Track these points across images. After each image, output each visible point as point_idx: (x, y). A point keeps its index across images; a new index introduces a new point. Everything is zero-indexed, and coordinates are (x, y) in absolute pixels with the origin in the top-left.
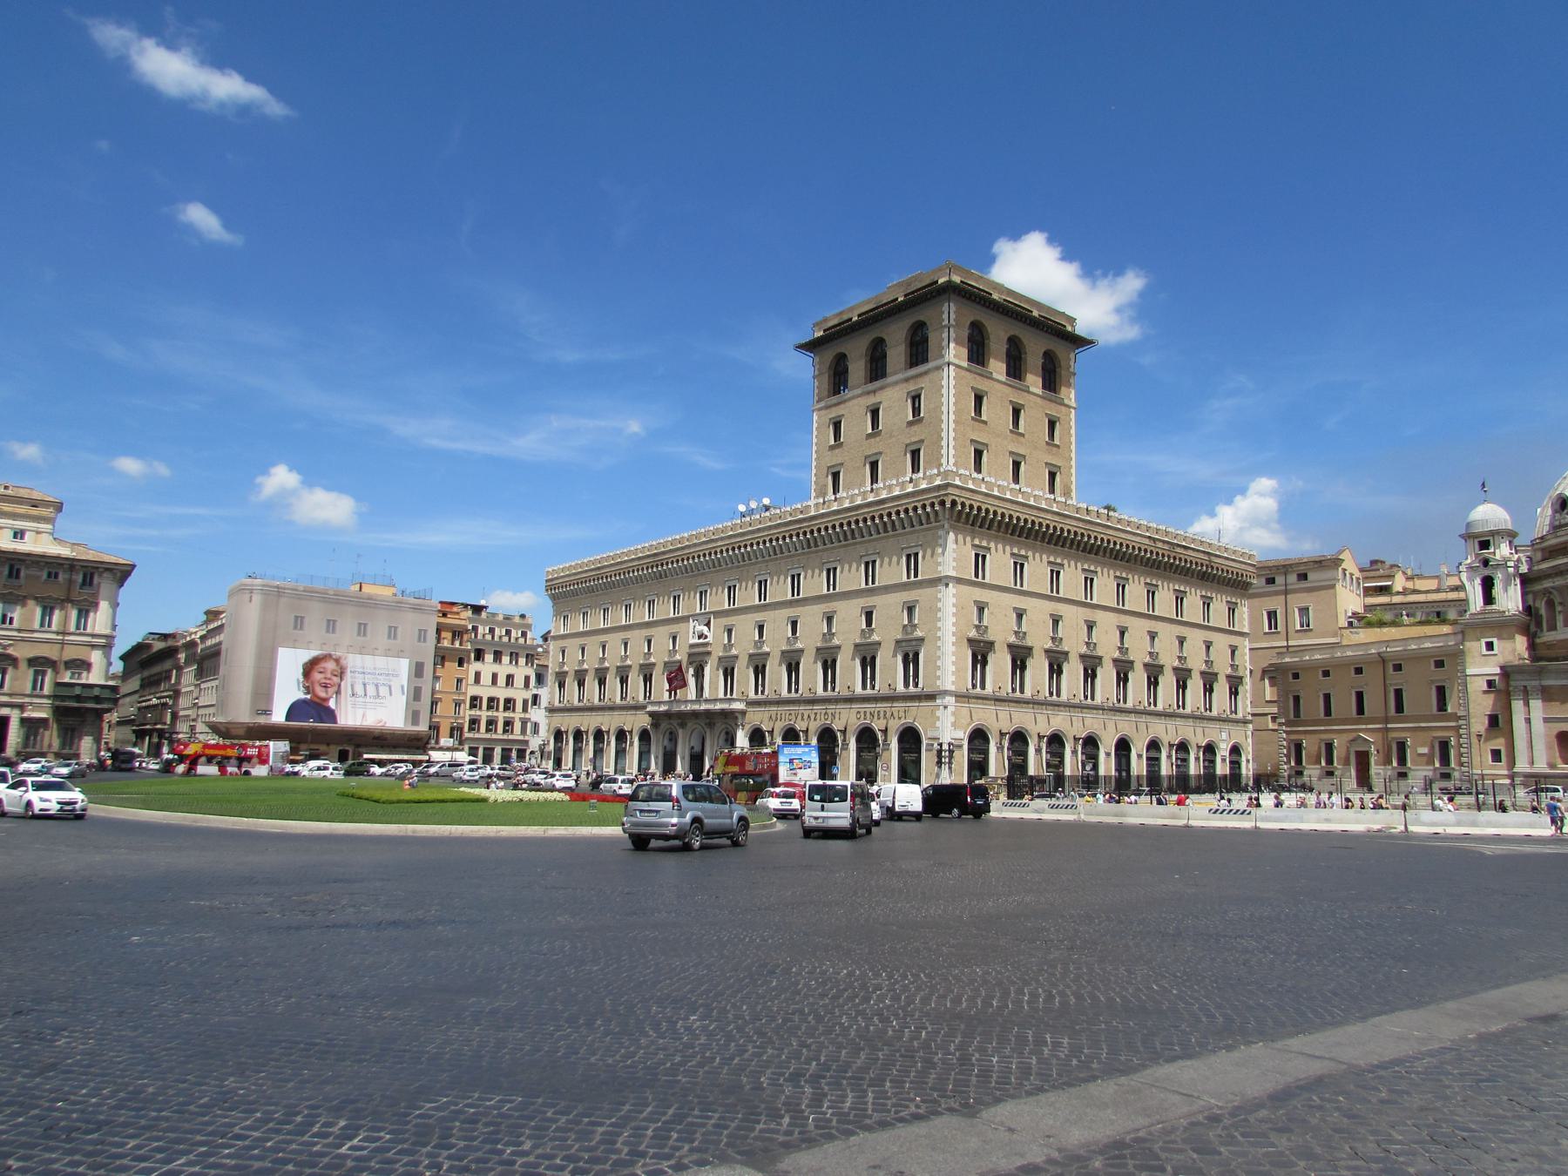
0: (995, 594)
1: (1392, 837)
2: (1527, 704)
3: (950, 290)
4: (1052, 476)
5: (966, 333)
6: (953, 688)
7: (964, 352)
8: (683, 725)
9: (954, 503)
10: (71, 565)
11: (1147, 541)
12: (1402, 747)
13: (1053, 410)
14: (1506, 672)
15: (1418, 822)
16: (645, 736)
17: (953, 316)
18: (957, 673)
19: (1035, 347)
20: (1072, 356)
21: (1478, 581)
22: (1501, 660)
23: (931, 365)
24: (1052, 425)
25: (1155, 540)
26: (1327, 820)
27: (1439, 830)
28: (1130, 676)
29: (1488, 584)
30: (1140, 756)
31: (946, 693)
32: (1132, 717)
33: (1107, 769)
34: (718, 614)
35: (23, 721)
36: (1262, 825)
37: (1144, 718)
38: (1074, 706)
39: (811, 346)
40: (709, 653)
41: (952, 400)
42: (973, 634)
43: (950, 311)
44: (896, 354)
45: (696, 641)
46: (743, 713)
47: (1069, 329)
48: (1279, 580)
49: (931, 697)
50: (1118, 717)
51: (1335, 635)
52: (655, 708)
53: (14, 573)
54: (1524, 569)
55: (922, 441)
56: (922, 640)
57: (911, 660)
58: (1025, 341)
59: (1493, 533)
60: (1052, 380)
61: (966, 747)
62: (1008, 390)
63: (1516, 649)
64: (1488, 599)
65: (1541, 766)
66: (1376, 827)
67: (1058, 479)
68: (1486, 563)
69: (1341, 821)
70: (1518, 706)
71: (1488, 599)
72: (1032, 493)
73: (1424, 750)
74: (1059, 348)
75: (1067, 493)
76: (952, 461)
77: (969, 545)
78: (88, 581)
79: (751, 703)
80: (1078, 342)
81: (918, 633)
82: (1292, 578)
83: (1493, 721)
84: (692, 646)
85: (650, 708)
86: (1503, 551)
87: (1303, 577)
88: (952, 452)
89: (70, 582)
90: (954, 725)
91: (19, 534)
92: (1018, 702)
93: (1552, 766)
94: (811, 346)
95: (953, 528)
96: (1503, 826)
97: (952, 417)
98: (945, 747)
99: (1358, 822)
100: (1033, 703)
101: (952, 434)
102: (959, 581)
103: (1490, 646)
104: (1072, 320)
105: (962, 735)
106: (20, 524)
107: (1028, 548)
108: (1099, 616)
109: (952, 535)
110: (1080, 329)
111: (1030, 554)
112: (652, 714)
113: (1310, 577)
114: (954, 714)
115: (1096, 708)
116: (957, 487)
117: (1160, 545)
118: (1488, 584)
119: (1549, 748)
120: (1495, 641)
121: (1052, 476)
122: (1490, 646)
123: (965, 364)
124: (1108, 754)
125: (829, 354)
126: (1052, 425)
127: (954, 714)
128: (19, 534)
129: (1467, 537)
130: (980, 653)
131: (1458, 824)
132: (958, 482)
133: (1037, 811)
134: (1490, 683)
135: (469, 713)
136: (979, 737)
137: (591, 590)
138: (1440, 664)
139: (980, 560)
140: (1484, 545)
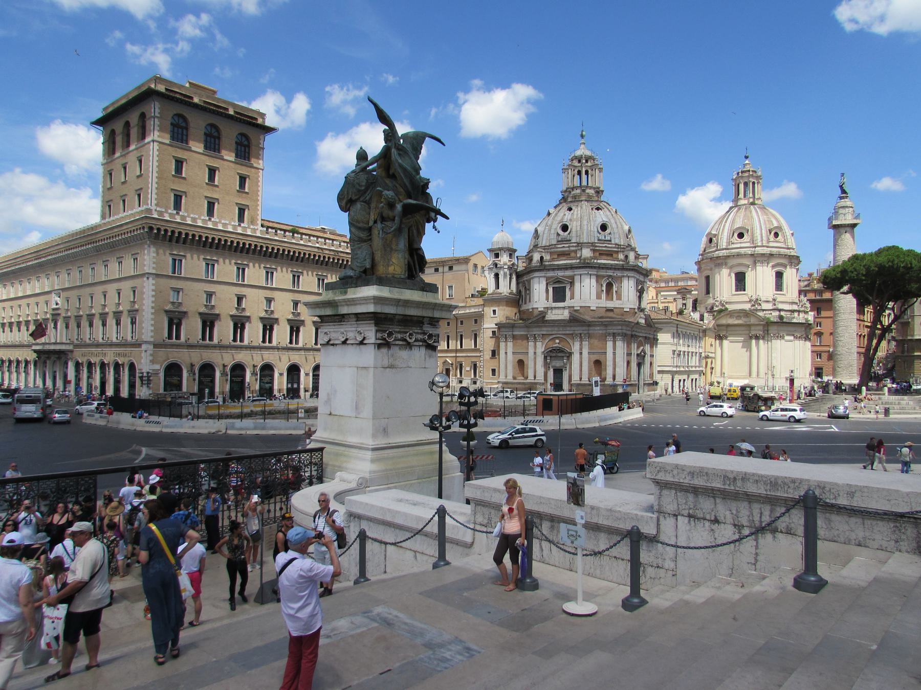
0: (189, 283)
1: (220, 436)
2: (506, 345)
3: (145, 96)
4: (241, 212)
6: (152, 340)
7: (168, 136)
8: (49, 358)
9: (151, 228)
11: (316, 250)
12: (461, 365)
13: (244, 171)
14: (500, 326)
15: (233, 428)
16: (35, 365)
17: (157, 110)
18: (157, 330)
19: (230, 133)
20: (262, 137)
21: (492, 275)
22: (497, 320)
23: (147, 140)
24: (243, 179)
25: (322, 249)
26: (193, 427)
27: (243, 432)
28: (301, 329)
29: (497, 276)
30: (307, 374)
31: (146, 342)
32: (302, 353)
33: (280, 383)
34: (63, 290)
36: (165, 430)
37: (311, 353)
38: (254, 348)
39: (100, 122)
40: (59, 314)
41: (156, 164)
42: (169, 307)
43: (154, 109)
44: (134, 132)
45: (55, 306)
46: (72, 351)
47: (260, 121)
48: (441, 269)
49: (138, 345)
50: (291, 353)
51: (463, 302)
52: (38, 348)
54: (520, 269)
55: (141, 189)
56: (137, 311)
57: (133, 323)
58: (221, 127)
59: (500, 249)
60: (246, 150)
61: (162, 375)
62: (203, 157)
63: (504, 313)
64: (497, 287)
65: (510, 378)
66: (213, 431)
67: (246, 213)
68: (496, 265)
69: (171, 427)
70: (502, 345)
71: (497, 287)
72: (225, 223)
73: (468, 369)
74: (250, 132)
75: (253, 221)
76: (154, 202)
77: (167, 254)
79: (76, 346)
80: (269, 130)
81: (136, 307)
82: (446, 269)
83: (494, 353)
84: (54, 309)
85: (34, 347)
86: (504, 259)
87: (451, 268)
88: (154, 196)
90: (153, 362)
92: (207, 347)
93: (514, 378)
94: (100, 122)
95: (154, 244)
96: (280, 429)
97: (155, 175)
98: (145, 374)
99: (206, 428)
100: (221, 347)
102: (157, 275)
103: (494, 311)
104: (263, 116)
105: (160, 368)
107: (217, 254)
108: (276, 295)
109: (153, 249)
110: (269, 123)
111: (221, 260)
112: (35, 351)
113: (455, 268)
114: (151, 355)
115: (273, 348)
116: (154, 218)
117: (327, 252)
118: (497, 276)
119: (514, 368)
120: (496, 309)
121: (241, 212)
122: (494, 311)
123: (168, 142)
124: (281, 374)
125: (109, 131)
126: (243, 179)
127: (151, 355)
129: (490, 250)
130: (175, 320)
131: (255, 428)
132: (155, 216)
133: (96, 420)
134: (494, 333)
136: (173, 370)
137: (13, 272)
138: (476, 321)
139: (176, 263)
140: (497, 256)
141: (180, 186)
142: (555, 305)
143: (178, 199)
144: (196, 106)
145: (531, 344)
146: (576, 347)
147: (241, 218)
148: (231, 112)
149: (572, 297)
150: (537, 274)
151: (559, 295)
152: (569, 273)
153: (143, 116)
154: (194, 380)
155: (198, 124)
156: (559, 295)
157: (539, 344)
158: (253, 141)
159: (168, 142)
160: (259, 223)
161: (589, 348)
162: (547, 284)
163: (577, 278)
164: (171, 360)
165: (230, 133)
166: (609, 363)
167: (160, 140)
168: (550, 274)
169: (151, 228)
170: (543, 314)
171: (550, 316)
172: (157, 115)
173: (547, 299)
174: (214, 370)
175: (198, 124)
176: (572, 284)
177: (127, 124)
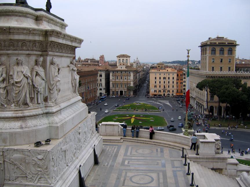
5: (211, 49)
10: (127, 71)
19: (226, 49)
35: (124, 91)
53: (121, 73)
58: (224, 48)
67: (231, 68)
74: (232, 48)
75: (232, 70)
76: (208, 70)
78: (130, 73)
89: (127, 73)
91: (121, 68)
101: (208, 66)
106: (121, 66)
121: (229, 68)
128: (121, 68)
135: (183, 87)
141: (213, 65)
143: (213, 68)
144: (217, 45)
147: (229, 70)
148: (227, 44)
153: (206, 48)
154: (216, 110)
155: (218, 49)
158: (233, 49)
159: (210, 55)
160: (235, 70)
164: (211, 105)
165: (226, 49)
167: (209, 55)
169: (207, 76)
172: (208, 49)
174: (222, 108)
175: (218, 49)
177: (204, 49)
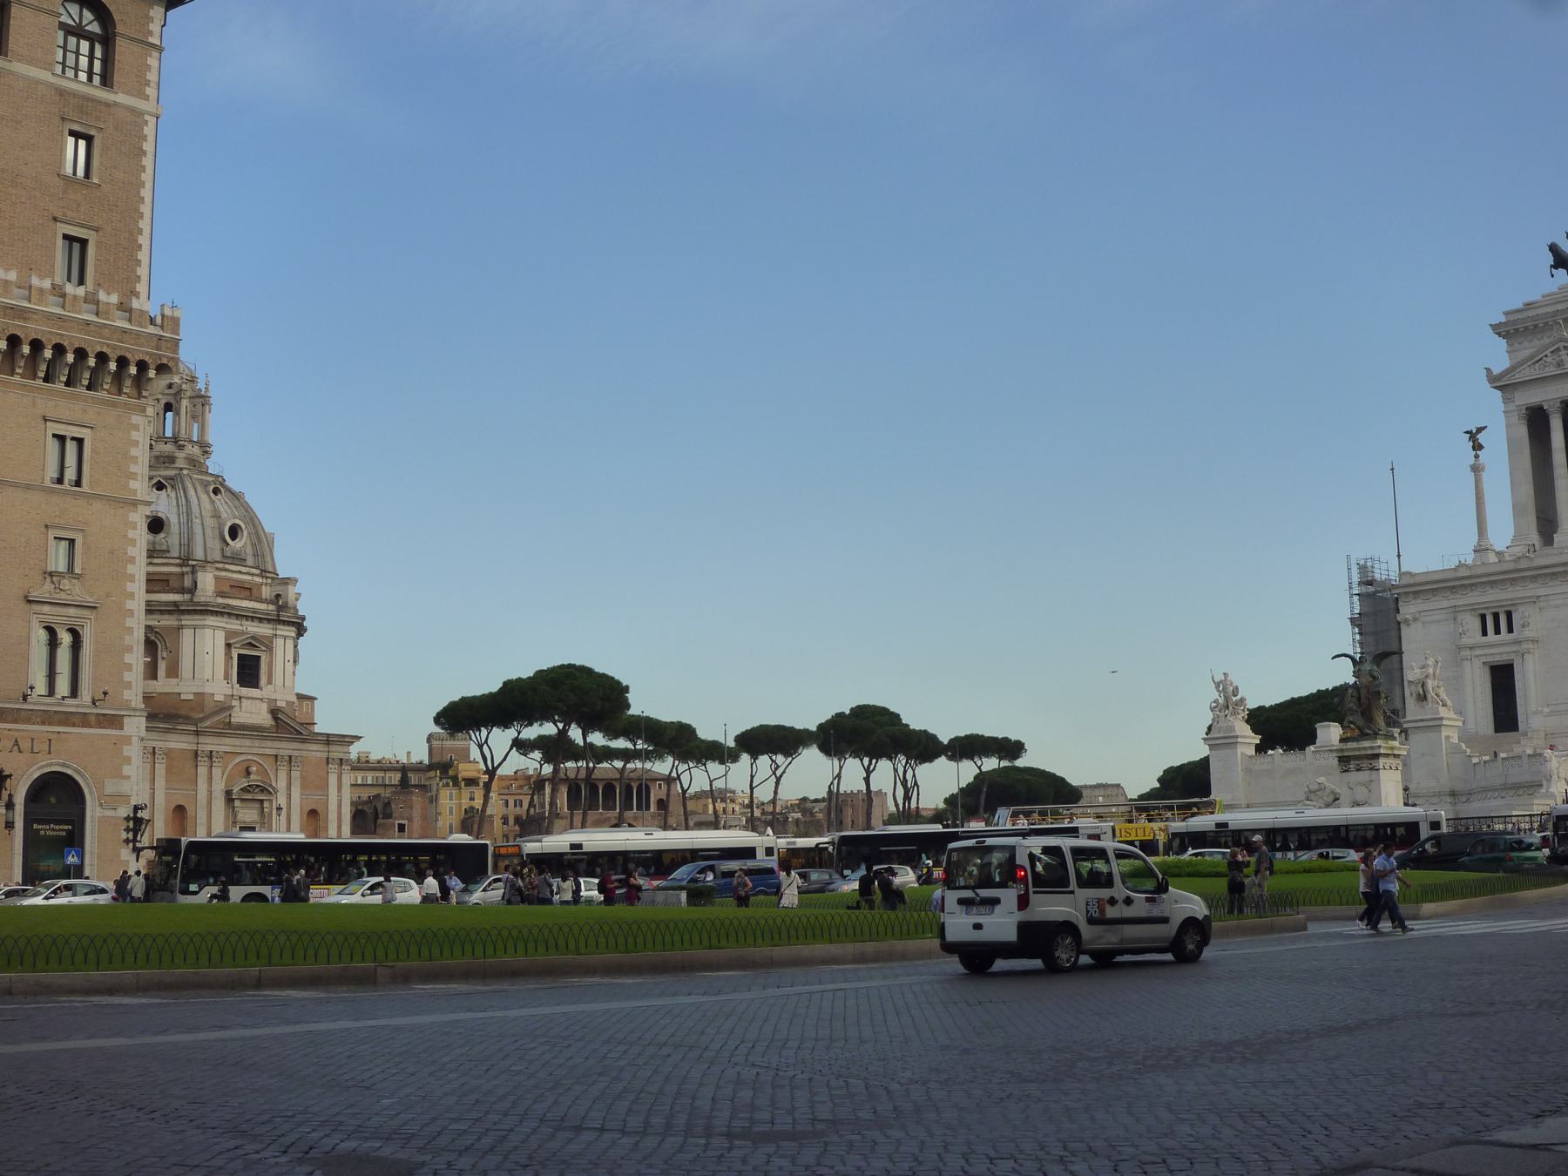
142: (245, 691)
145: (202, 770)
146: (281, 784)
149: (270, 682)
150: (211, 621)
151: (248, 671)
152: (264, 630)
156: (248, 671)
157: (217, 772)
161: (303, 786)
162: (228, 646)
163: (279, 643)
166: (333, 816)
168: (234, 625)
170: (225, 708)
171: (240, 716)
173: (227, 677)
176: (270, 649)
